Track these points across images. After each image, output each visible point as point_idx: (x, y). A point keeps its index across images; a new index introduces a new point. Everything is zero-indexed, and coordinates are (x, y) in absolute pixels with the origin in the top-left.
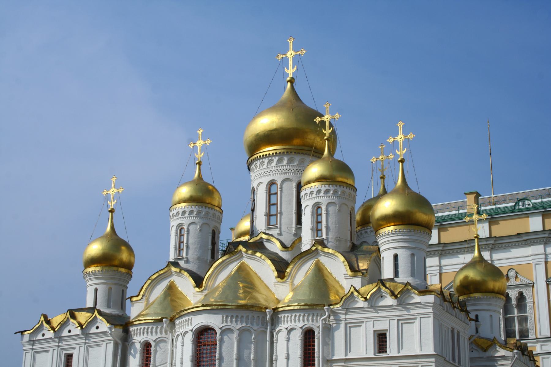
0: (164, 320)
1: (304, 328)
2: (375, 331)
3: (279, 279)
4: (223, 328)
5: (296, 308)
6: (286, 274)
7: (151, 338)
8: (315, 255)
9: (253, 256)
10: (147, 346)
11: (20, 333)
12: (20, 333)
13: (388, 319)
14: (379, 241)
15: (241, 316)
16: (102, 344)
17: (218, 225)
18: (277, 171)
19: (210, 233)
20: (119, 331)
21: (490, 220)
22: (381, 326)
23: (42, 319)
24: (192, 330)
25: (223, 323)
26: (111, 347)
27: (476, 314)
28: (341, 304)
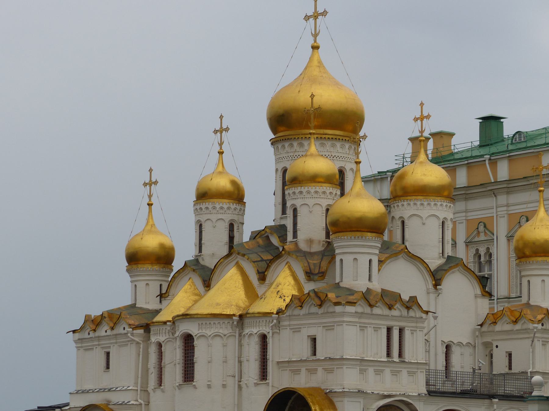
0: (168, 323)
1: (258, 334)
2: (308, 336)
3: (261, 281)
5: (252, 315)
6: (265, 277)
7: (161, 339)
8: (285, 258)
10: (160, 345)
11: (72, 332)
12: (72, 332)
13: (317, 326)
14: (334, 243)
15: (213, 323)
16: (128, 344)
17: (236, 218)
18: (288, 158)
19: (225, 228)
20: (141, 331)
22: (312, 332)
24: (178, 336)
25: (199, 330)
26: (134, 346)
27: (528, 280)
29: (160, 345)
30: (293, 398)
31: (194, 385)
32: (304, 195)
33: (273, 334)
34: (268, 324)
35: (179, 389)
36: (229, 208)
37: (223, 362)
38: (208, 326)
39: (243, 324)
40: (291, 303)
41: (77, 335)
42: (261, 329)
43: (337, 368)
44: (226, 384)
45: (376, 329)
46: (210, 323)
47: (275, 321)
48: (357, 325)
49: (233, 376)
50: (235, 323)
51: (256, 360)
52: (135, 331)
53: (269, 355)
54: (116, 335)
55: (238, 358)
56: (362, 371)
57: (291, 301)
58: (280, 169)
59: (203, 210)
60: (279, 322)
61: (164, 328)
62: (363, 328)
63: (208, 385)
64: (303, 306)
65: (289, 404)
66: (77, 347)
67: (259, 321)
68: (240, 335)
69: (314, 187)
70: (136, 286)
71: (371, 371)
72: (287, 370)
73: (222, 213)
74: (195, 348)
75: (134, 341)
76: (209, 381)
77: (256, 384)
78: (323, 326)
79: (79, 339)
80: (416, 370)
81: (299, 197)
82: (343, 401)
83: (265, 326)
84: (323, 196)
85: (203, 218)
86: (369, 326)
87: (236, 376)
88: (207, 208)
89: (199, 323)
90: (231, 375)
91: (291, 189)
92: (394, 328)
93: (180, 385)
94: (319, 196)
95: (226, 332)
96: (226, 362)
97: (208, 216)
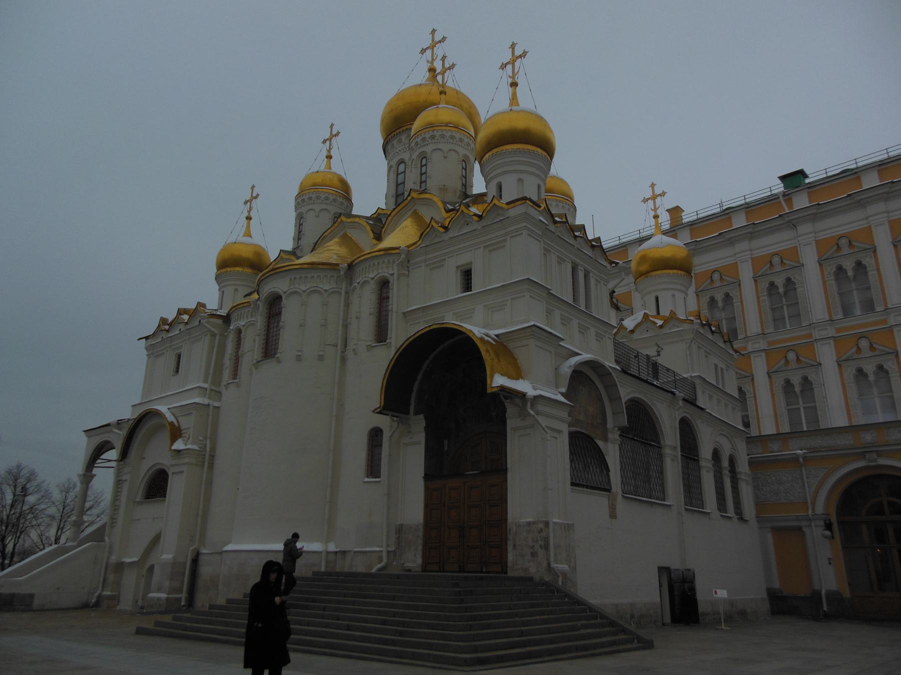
1: (376, 278)
2: (457, 267)
4: (290, 291)
6: (382, 235)
9: (354, 224)
11: (144, 339)
20: (220, 321)
21: (692, 227)
23: (161, 322)
26: (207, 339)
28: (421, 241)
29: (239, 331)
30: (431, 357)
31: (278, 357)
32: (437, 139)
33: (399, 276)
34: (391, 265)
35: (256, 369)
36: (334, 200)
37: (322, 325)
38: (303, 281)
39: (351, 279)
40: (429, 229)
41: (149, 341)
42: (380, 271)
43: (512, 299)
44: (323, 355)
45: (561, 261)
46: (306, 277)
47: (403, 256)
48: (540, 241)
49: (334, 345)
50: (342, 273)
51: (370, 314)
52: (211, 320)
53: (392, 305)
54: (189, 329)
55: (343, 321)
56: (549, 312)
57: (430, 227)
58: (394, 166)
59: (306, 200)
60: (409, 261)
61: (246, 311)
62: (546, 251)
63: (297, 355)
64: (449, 227)
65: (424, 367)
66: (147, 355)
67: (379, 264)
68: (347, 293)
69: (450, 132)
70: (223, 292)
71: (557, 314)
72: (420, 322)
73: (327, 204)
74: (283, 310)
75: (209, 330)
76: (298, 351)
77: (370, 348)
78: (485, 247)
79: (150, 345)
80: (604, 334)
81: (430, 142)
82: (528, 345)
83: (387, 267)
84: (459, 143)
85: (303, 210)
86: (552, 250)
87: (339, 345)
88: (310, 198)
89: (291, 279)
90: (331, 343)
91: (419, 136)
92: (579, 267)
93: (258, 362)
94: (455, 142)
95: (327, 288)
96: (325, 326)
97: (310, 207)
